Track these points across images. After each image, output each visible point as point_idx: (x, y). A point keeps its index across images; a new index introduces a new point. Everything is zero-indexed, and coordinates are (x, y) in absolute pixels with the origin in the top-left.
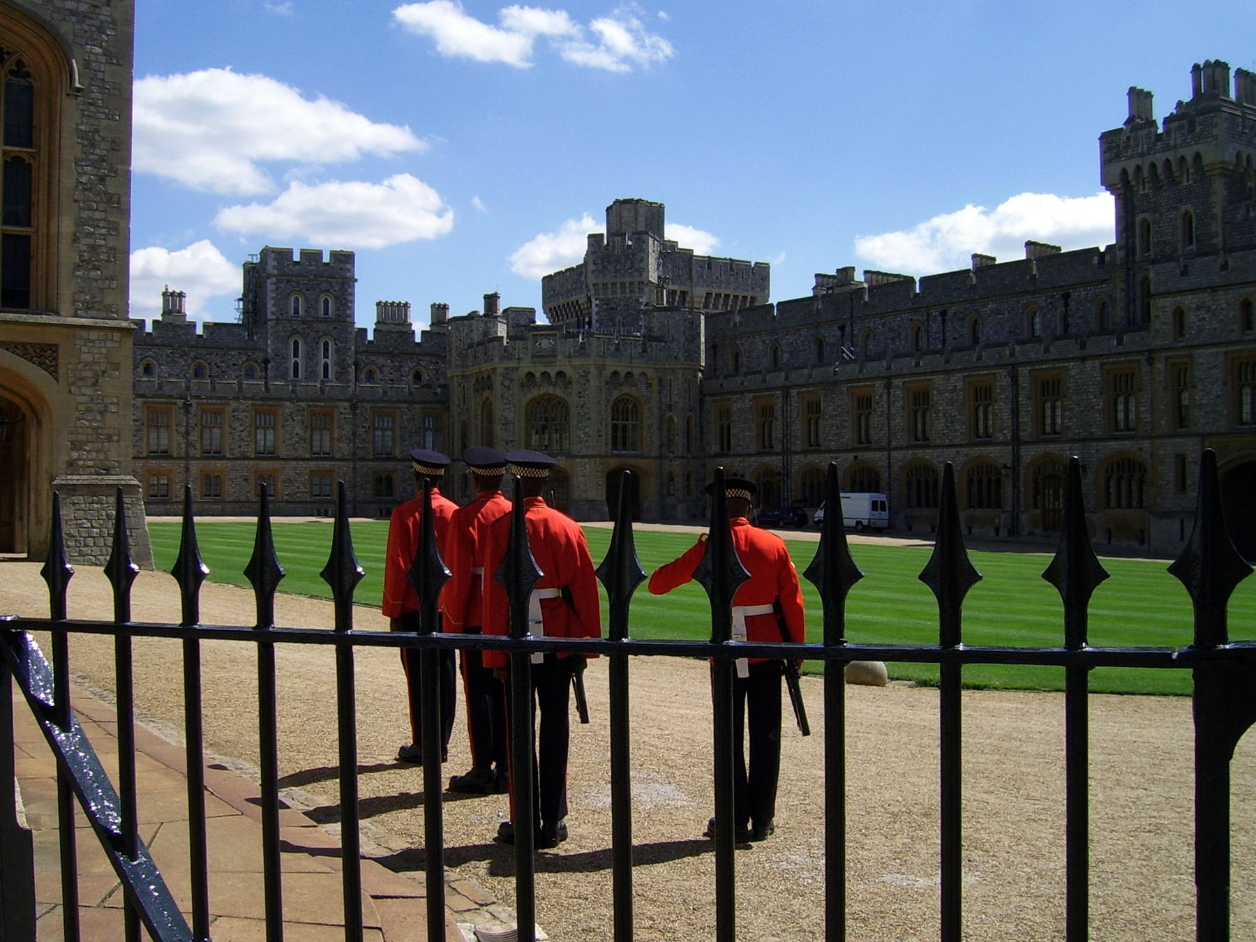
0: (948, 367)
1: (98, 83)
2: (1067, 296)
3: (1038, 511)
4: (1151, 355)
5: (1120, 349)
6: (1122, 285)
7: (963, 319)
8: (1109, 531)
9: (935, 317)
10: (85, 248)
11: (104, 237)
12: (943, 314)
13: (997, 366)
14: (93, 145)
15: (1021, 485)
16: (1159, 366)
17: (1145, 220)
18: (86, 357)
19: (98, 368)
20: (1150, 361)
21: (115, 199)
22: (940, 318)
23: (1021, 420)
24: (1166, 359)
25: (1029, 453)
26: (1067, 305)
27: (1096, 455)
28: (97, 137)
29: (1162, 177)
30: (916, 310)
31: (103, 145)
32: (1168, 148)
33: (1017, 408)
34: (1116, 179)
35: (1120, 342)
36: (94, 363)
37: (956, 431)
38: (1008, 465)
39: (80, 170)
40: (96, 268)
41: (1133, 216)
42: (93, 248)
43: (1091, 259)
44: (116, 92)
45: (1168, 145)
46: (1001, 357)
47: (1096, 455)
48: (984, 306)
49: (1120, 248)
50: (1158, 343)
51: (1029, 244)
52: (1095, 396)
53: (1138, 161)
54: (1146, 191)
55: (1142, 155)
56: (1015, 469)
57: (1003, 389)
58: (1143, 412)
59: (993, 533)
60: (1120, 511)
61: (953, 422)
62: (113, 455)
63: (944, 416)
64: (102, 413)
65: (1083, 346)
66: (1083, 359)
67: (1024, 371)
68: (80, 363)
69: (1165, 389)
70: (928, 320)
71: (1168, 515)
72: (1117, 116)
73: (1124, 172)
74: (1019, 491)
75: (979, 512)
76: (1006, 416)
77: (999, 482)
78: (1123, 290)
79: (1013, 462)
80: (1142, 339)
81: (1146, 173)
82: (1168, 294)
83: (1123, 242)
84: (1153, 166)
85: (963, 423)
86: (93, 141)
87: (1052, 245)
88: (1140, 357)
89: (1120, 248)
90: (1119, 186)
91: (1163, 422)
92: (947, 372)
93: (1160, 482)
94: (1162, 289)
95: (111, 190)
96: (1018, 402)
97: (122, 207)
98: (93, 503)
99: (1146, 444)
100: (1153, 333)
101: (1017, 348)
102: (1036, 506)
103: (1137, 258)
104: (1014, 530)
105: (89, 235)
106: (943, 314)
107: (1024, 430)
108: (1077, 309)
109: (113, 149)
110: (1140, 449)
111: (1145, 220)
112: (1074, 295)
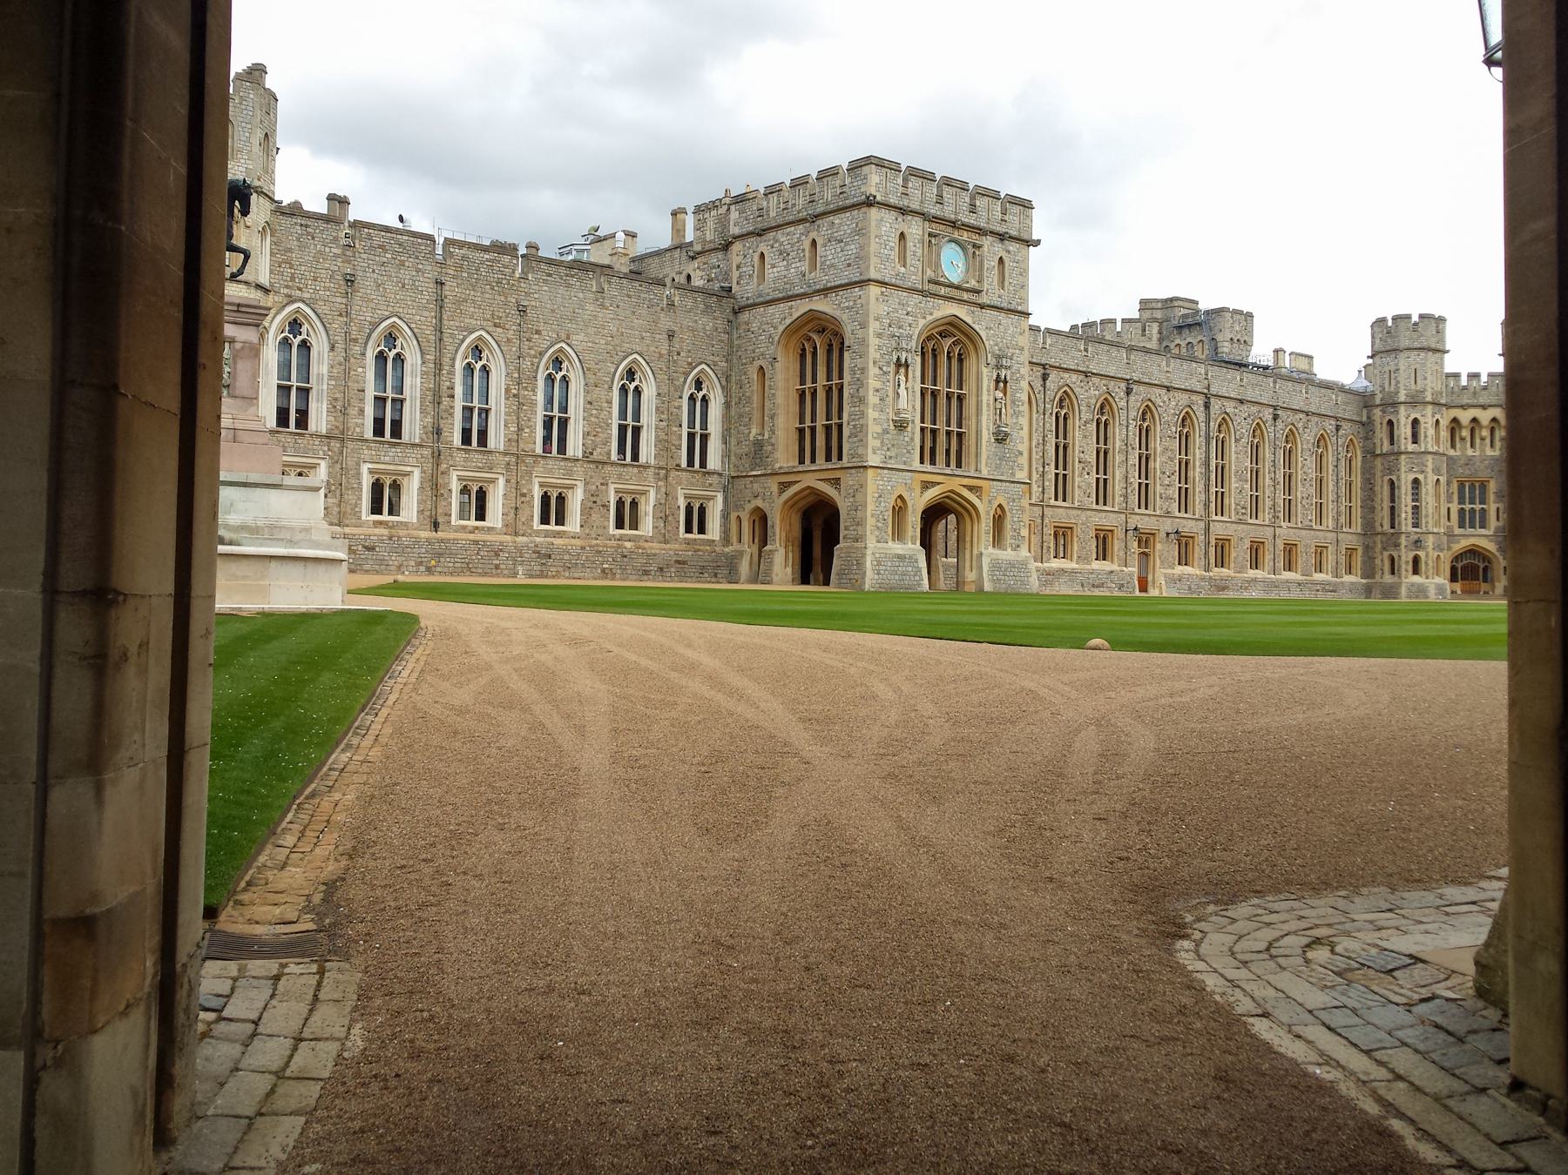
18: (851, 483)
64: (856, 510)
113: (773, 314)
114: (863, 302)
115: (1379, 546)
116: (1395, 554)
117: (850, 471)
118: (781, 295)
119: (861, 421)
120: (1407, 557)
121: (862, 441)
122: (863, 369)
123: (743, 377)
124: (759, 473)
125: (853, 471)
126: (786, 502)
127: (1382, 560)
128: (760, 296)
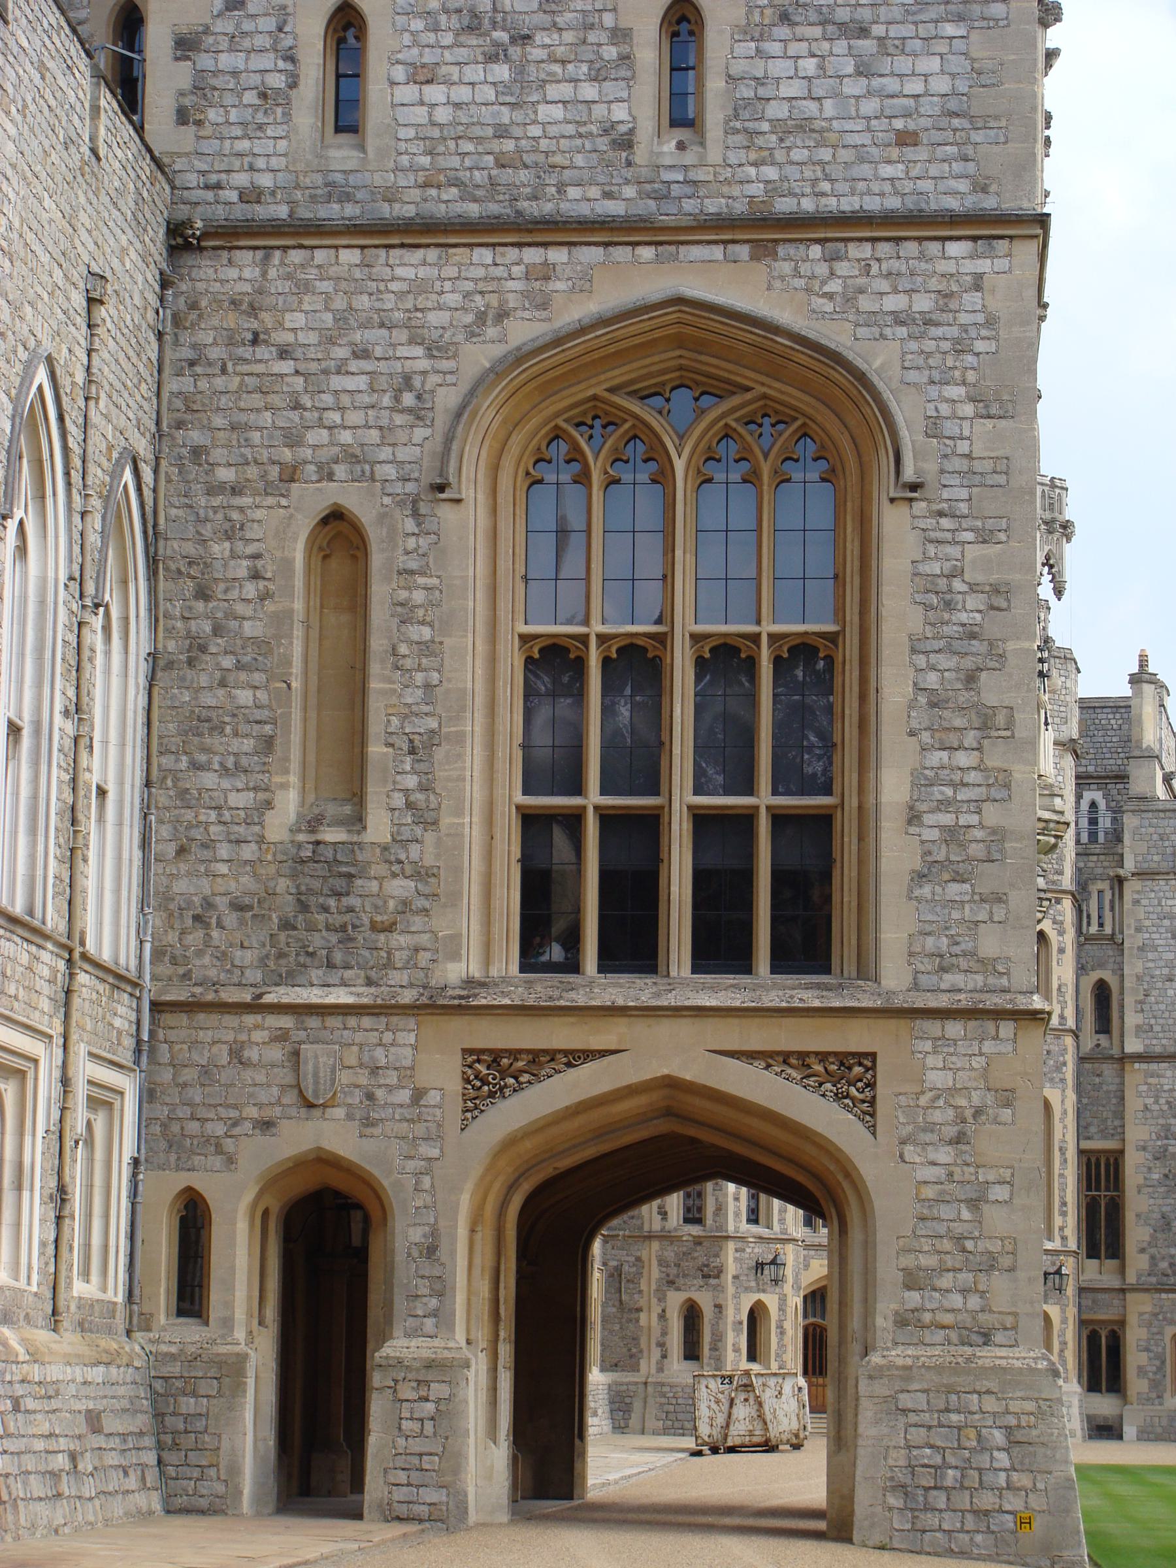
1: (958, 464)
10: (934, 834)
11: (977, 806)
14: (949, 605)
18: (938, 1079)
19: (962, 1102)
21: (1001, 719)
28: (958, 585)
31: (973, 602)
36: (953, 1091)
39: (921, 661)
40: (959, 878)
42: (952, 835)
44: (1001, 479)
62: (1001, 1300)
64: (974, 1204)
68: (923, 1093)
86: (948, 597)
95: (990, 698)
97: (1016, 735)
98: (948, 1410)
105: (943, 805)
109: (993, 608)
113: (419, 287)
114: (993, 305)
115: (656, 1273)
116: (705, 1300)
117: (933, 1027)
118: (473, 210)
119: (992, 815)
120: (738, 1310)
121: (999, 899)
122: (996, 590)
123: (220, 549)
124: (341, 996)
125: (954, 1029)
126: (510, 1142)
127: (662, 1316)
128: (341, 193)
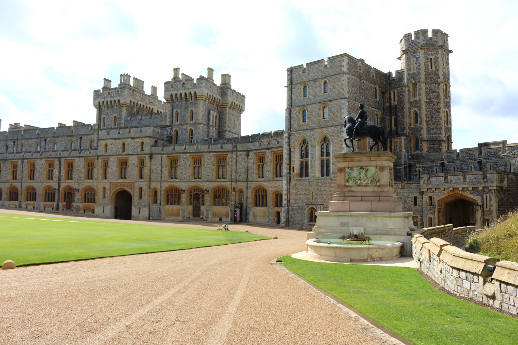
0: (41, 157)
2: (81, 138)
3: (65, 203)
4: (98, 156)
5: (90, 155)
6: (96, 136)
7: (51, 142)
8: (84, 209)
9: (43, 141)
12: (45, 140)
13: (55, 158)
15: (60, 195)
16: (100, 160)
17: (104, 118)
20: (98, 159)
22: (44, 142)
23: (61, 175)
24: (102, 158)
25: (63, 185)
26: (81, 140)
27: (82, 186)
29: (109, 105)
30: (37, 138)
32: (111, 97)
33: (60, 171)
34: (97, 104)
35: (90, 153)
37: (42, 177)
38: (57, 189)
41: (101, 116)
43: (89, 127)
45: (111, 96)
46: (57, 155)
47: (82, 186)
48: (57, 139)
49: (97, 125)
50: (99, 154)
51: (74, 121)
52: (82, 169)
53: (103, 100)
54: (105, 109)
55: (104, 98)
56: (59, 190)
57: (57, 165)
58: (95, 174)
59: (51, 209)
60: (88, 204)
61: (41, 174)
63: (39, 172)
65: (80, 153)
66: (80, 157)
67: (63, 160)
69: (101, 167)
70: (41, 142)
71: (100, 205)
72: (100, 87)
73: (99, 103)
74: (59, 197)
75: (48, 203)
76: (57, 173)
77: (54, 194)
78: (97, 137)
79: (58, 188)
80: (96, 152)
81: (105, 103)
82: (103, 139)
83: (98, 123)
84: (107, 102)
85: (44, 175)
87: (82, 122)
88: (95, 158)
89: (97, 125)
90: (98, 106)
91: (100, 177)
92: (41, 158)
93: (98, 195)
94: (102, 138)
96: (61, 169)
99: (95, 184)
100: (99, 151)
101: (61, 152)
102: (65, 201)
103: (101, 128)
104: (57, 209)
106: (45, 140)
107: (62, 178)
108: (84, 142)
110: (94, 185)
111: (104, 118)
112: (83, 138)
